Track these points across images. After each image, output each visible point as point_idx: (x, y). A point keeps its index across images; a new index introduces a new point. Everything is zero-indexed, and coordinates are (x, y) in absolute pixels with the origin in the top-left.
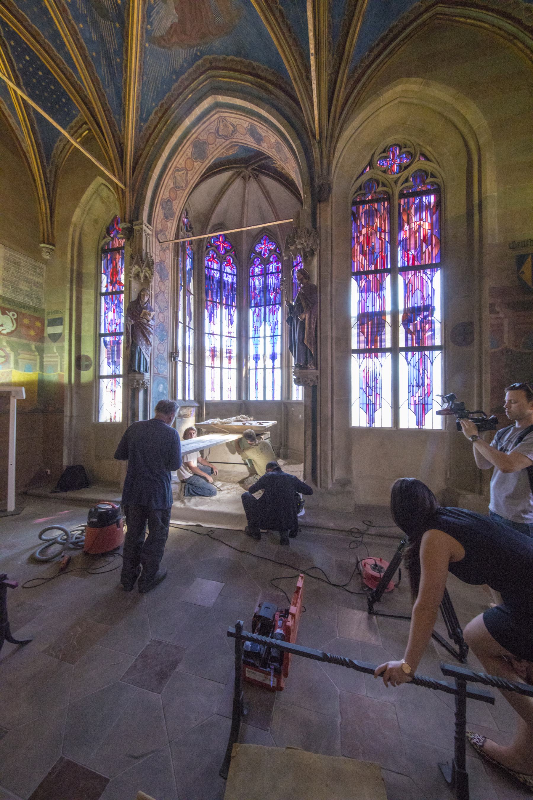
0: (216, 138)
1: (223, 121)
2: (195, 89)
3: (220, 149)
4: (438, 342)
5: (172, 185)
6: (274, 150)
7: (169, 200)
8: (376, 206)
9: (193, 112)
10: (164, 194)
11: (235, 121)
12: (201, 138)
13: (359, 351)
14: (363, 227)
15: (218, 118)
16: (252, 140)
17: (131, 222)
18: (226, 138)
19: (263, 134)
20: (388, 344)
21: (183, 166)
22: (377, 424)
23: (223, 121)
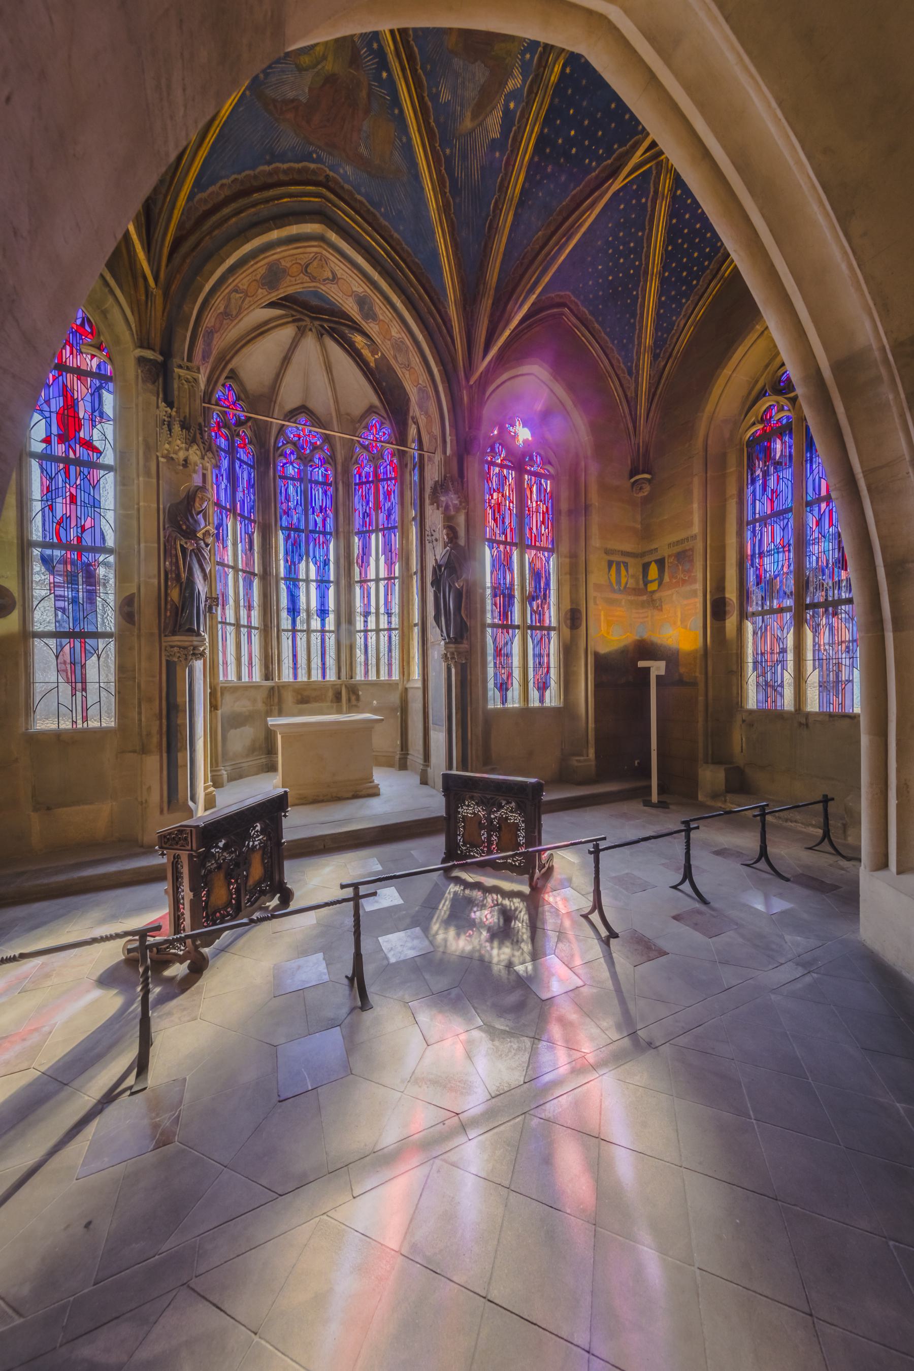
0: (302, 272)
1: (321, 260)
2: (297, 197)
3: (298, 286)
4: (554, 624)
5: (222, 309)
6: (389, 342)
7: (211, 331)
8: (505, 471)
9: (288, 228)
10: (209, 320)
11: (339, 273)
12: (283, 263)
13: (493, 626)
14: (494, 491)
15: (316, 253)
16: (356, 308)
17: (161, 354)
18: (313, 279)
19: (381, 317)
20: (517, 620)
21: (245, 287)
22: (509, 705)
23: (321, 260)
